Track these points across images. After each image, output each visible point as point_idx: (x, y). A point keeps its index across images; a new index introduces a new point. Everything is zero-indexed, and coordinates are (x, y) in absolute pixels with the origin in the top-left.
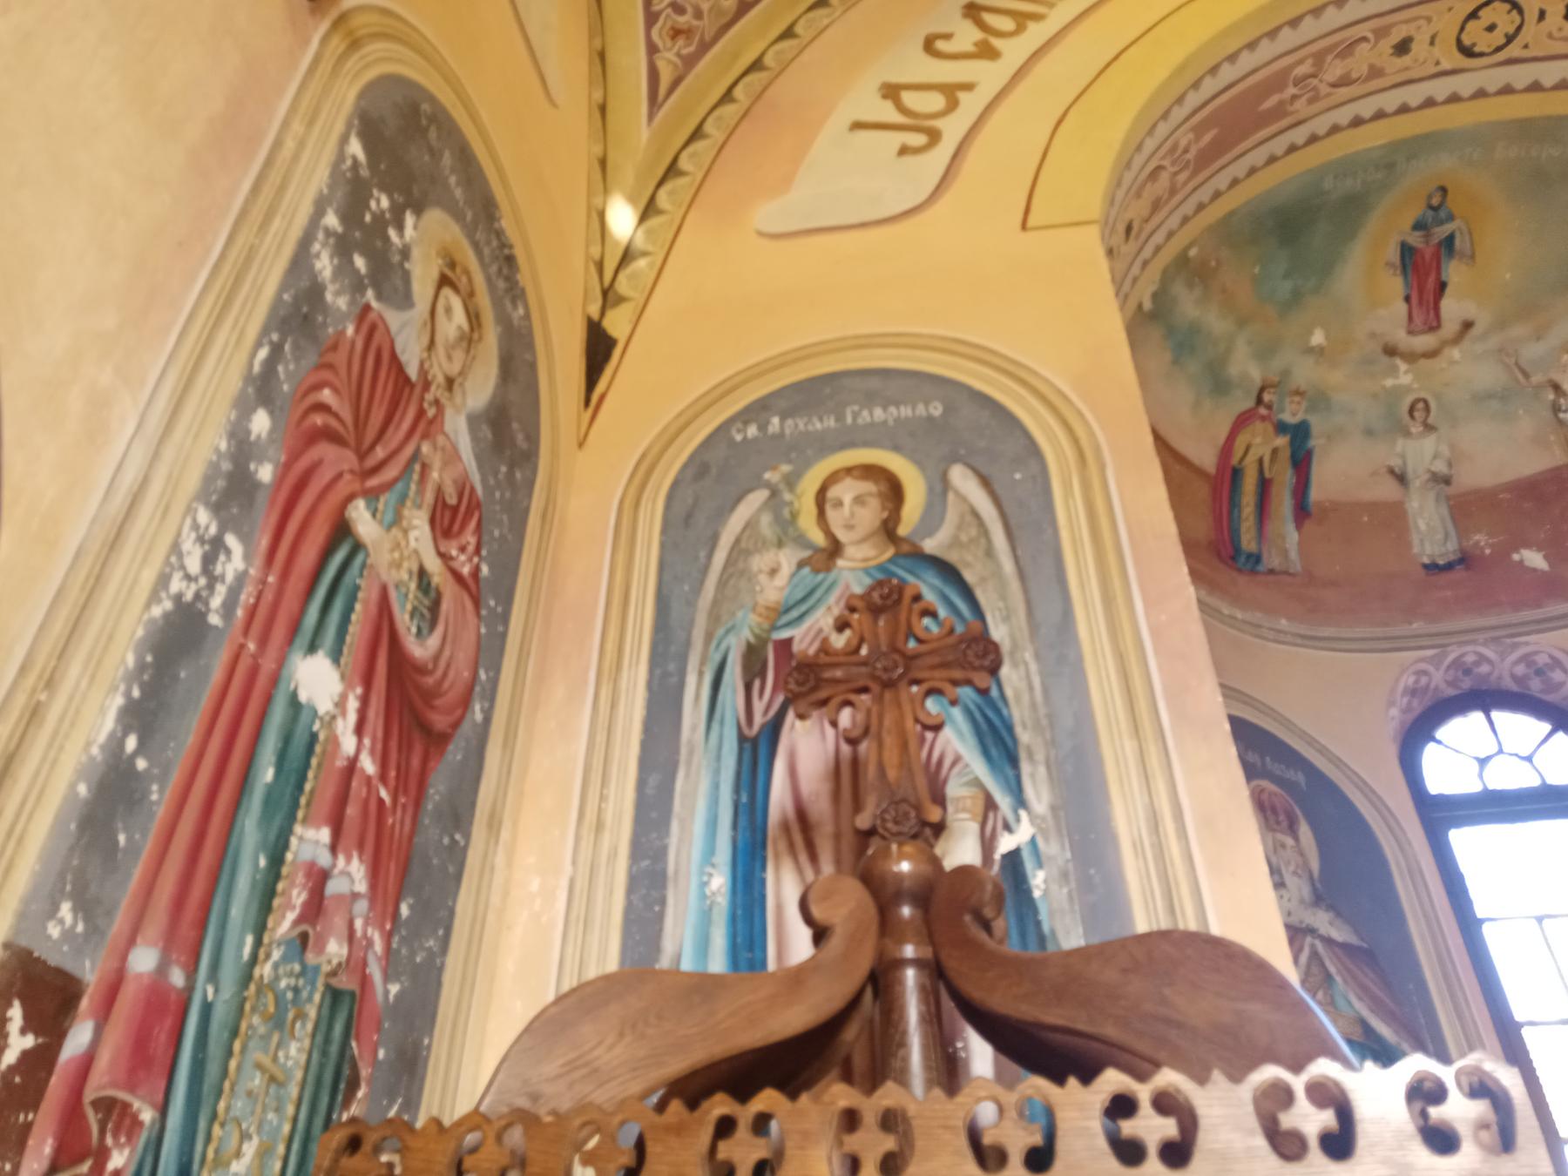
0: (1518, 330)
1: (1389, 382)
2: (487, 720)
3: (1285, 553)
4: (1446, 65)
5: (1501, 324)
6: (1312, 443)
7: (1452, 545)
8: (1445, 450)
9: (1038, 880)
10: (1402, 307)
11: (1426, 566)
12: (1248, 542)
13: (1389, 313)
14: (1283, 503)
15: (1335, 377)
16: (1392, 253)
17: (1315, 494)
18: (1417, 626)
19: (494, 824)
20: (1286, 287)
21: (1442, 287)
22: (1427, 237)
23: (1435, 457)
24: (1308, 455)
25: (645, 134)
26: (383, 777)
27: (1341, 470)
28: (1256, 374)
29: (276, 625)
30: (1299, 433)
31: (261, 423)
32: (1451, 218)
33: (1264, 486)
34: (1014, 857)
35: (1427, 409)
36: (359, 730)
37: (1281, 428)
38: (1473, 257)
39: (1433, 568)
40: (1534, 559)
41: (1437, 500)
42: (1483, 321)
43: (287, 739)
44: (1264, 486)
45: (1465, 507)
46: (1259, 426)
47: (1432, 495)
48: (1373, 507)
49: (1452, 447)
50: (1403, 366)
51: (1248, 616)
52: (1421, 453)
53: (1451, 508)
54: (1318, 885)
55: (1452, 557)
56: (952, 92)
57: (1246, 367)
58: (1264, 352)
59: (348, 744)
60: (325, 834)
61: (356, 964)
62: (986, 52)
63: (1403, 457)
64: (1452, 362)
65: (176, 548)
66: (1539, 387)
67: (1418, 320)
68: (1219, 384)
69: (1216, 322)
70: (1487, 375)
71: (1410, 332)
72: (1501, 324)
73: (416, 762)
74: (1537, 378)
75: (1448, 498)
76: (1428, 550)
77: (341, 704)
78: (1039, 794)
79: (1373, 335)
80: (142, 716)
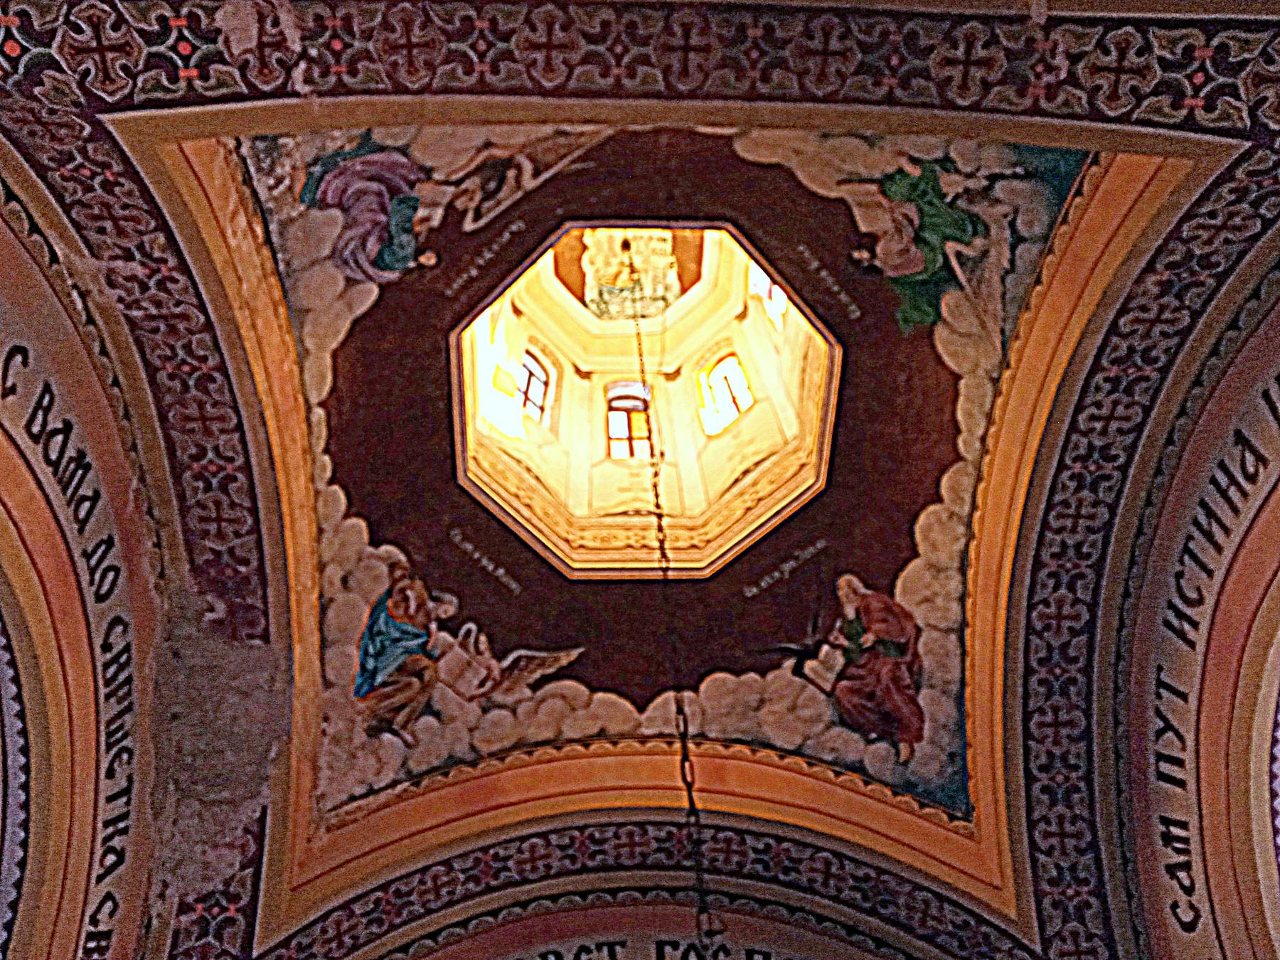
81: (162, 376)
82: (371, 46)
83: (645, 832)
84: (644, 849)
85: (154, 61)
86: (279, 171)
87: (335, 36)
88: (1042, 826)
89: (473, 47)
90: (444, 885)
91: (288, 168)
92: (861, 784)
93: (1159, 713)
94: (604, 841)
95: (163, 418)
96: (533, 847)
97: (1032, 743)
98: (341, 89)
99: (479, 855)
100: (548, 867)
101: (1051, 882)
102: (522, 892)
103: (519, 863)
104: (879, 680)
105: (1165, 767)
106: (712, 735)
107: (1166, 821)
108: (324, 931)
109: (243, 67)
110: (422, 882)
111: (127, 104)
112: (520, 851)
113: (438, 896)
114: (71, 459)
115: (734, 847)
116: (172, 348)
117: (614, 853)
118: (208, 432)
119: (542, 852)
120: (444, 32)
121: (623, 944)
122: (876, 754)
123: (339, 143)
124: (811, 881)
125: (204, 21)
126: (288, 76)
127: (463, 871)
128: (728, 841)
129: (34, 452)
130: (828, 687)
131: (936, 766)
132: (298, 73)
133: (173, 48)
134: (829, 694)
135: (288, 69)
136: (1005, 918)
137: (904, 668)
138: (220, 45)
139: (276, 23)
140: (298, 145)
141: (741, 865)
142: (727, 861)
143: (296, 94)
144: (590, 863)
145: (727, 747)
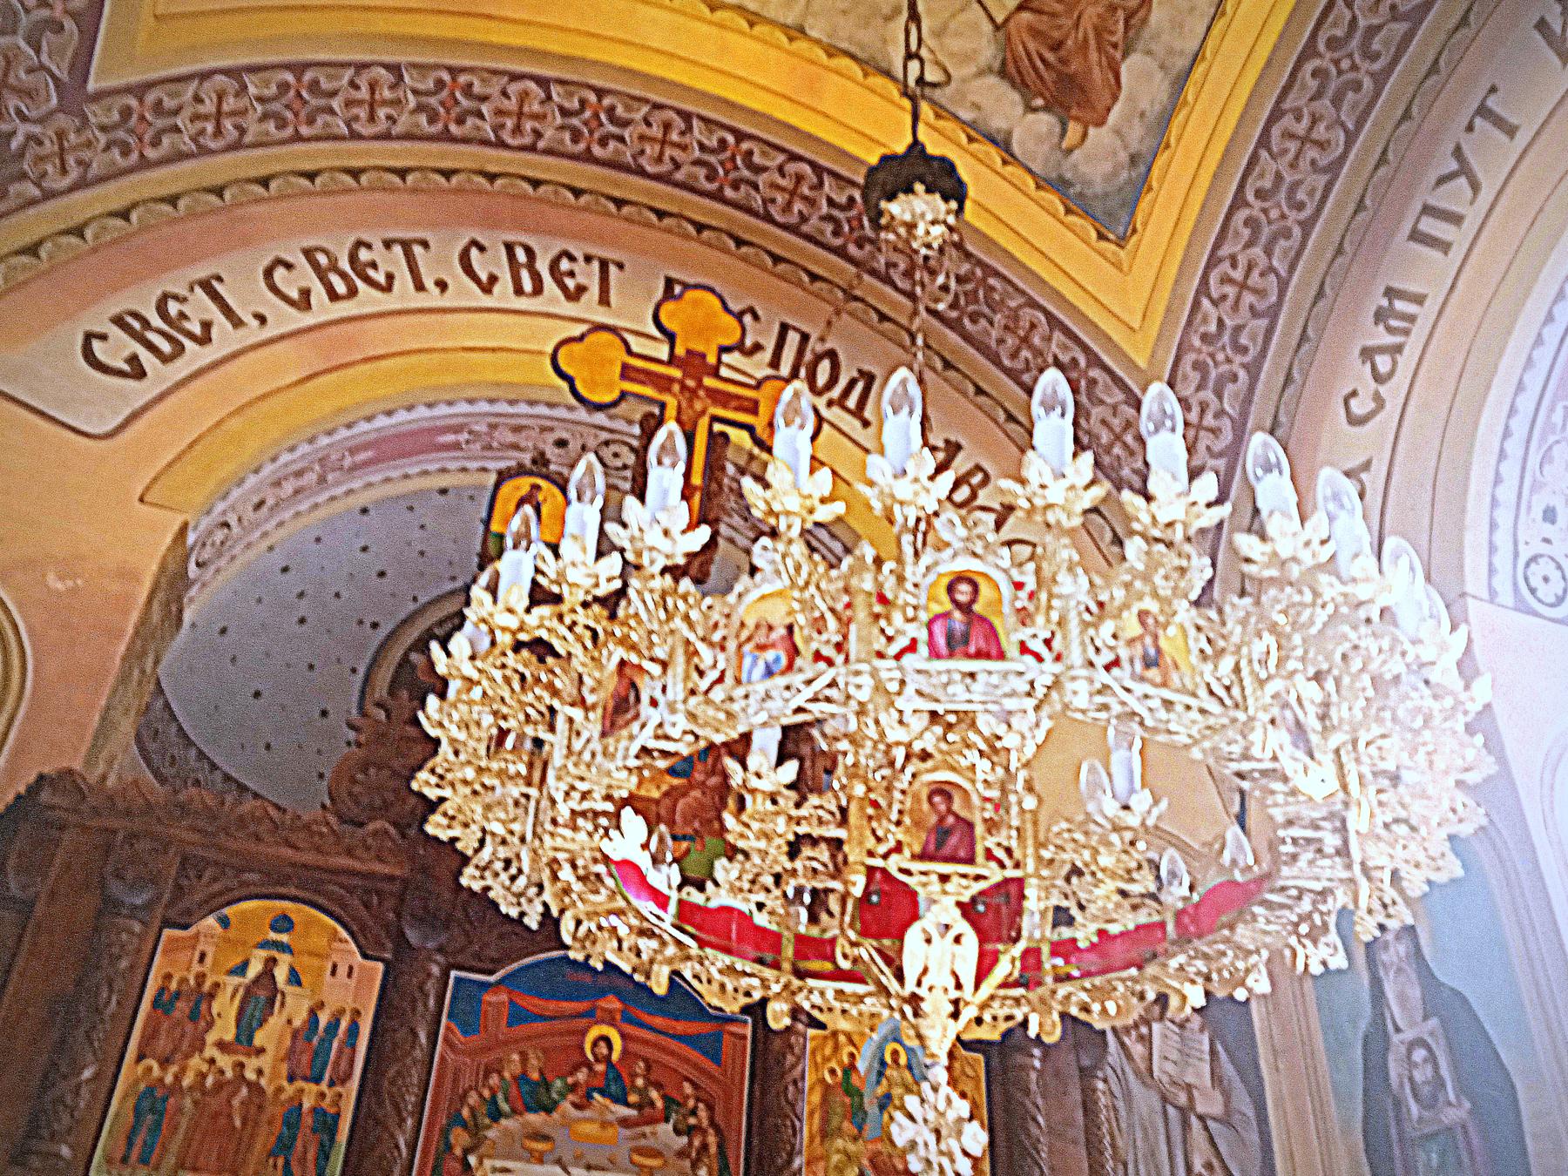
83: (689, 128)
84: (677, 153)
88: (1225, 266)
90: (385, 103)
92: (999, 161)
93: (1458, 152)
94: (625, 124)
96: (524, 96)
97: (1264, 154)
99: (446, 77)
100: (538, 134)
101: (1205, 338)
102: (495, 159)
103: (499, 112)
104: (1077, 25)
105: (1429, 225)
106: (814, 34)
107: (1390, 293)
108: (198, 99)
110: (354, 85)
112: (505, 94)
113: (372, 118)
115: (806, 191)
117: (637, 147)
119: (536, 108)
121: (620, 266)
122: (1034, 130)
124: (891, 265)
127: (415, 92)
128: (799, 178)
130: (1000, 19)
131: (1107, 167)
134: (997, 27)
136: (1131, 365)
137: (1121, 15)
141: (804, 219)
142: (787, 207)
144: (597, 150)
145: (830, 55)
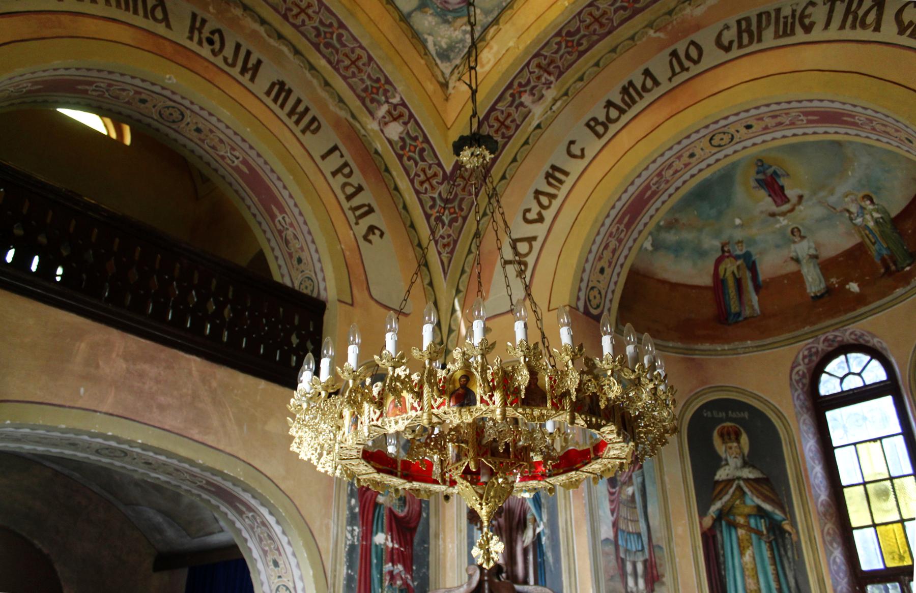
0: (822, 194)
1: (778, 226)
2: (428, 514)
3: (752, 307)
4: (713, 152)
5: (814, 193)
6: (753, 258)
7: (823, 286)
8: (813, 245)
9: (544, 539)
10: (769, 200)
11: (812, 297)
12: (734, 307)
13: (766, 202)
14: (749, 285)
15: (754, 231)
16: (753, 183)
17: (761, 278)
18: (807, 329)
19: (437, 536)
20: (713, 212)
21: (782, 188)
22: (764, 173)
23: (809, 248)
24: (754, 263)
25: (445, 285)
26: (401, 546)
27: (771, 264)
28: (717, 243)
29: (367, 535)
30: (747, 257)
31: (353, 501)
32: (770, 166)
33: (739, 282)
34: (539, 534)
35: (799, 231)
36: (392, 541)
37: (737, 258)
38: (788, 175)
39: (816, 298)
40: (854, 287)
41: (814, 266)
42: (806, 193)
43: (377, 553)
44: (739, 282)
45: (827, 266)
46: (727, 260)
47: (812, 265)
48: (786, 276)
49: (815, 242)
50: (781, 219)
51: (732, 346)
52: (803, 248)
53: (821, 269)
54: (746, 458)
55: (823, 291)
56: (531, 240)
57: (712, 243)
58: (717, 234)
59: (390, 545)
60: (390, 564)
61: (405, 583)
62: (540, 219)
63: (796, 252)
64: (801, 211)
65: (346, 537)
66: (841, 211)
67: (779, 201)
68: (702, 253)
69: (687, 235)
70: (819, 212)
71: (778, 206)
72: (814, 193)
73: (409, 537)
74: (839, 209)
75: (819, 264)
76: (813, 290)
77: (386, 539)
78: (545, 517)
79: (762, 212)
80: (350, 567)
81: (581, 48)
82: (365, 77)
85: (423, 160)
86: (460, 36)
87: (372, 93)
89: (332, 38)
91: (457, 33)
95: (609, 32)
98: (388, 81)
109: (405, 124)
111: (440, 165)
114: (623, 100)
116: (561, 57)
118: (605, 13)
120: (337, 53)
123: (430, 18)
125: (401, 144)
126: (398, 104)
129: (613, 128)
132: (396, 100)
133: (414, 152)
135: (395, 107)
138: (404, 135)
139: (384, 117)
140: (443, 37)
143: (401, 99)
